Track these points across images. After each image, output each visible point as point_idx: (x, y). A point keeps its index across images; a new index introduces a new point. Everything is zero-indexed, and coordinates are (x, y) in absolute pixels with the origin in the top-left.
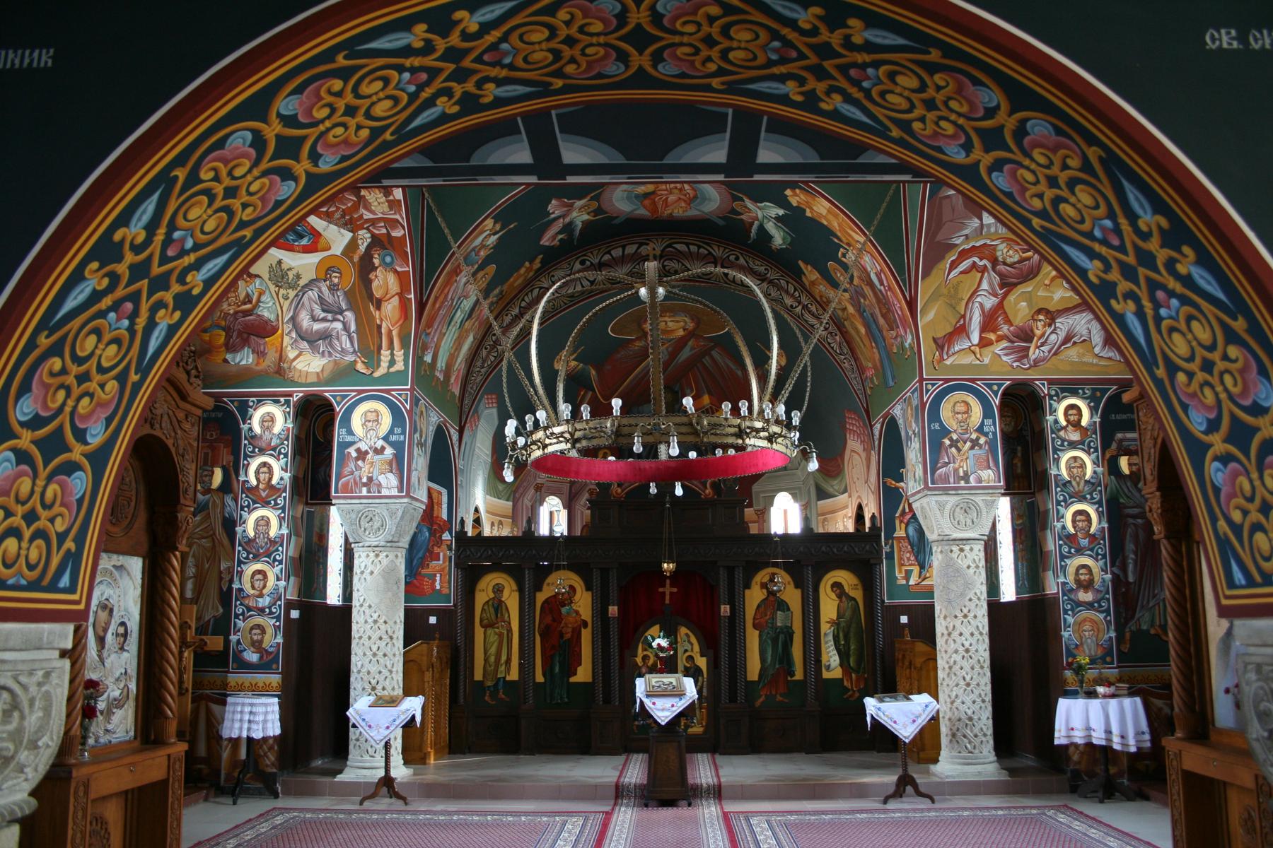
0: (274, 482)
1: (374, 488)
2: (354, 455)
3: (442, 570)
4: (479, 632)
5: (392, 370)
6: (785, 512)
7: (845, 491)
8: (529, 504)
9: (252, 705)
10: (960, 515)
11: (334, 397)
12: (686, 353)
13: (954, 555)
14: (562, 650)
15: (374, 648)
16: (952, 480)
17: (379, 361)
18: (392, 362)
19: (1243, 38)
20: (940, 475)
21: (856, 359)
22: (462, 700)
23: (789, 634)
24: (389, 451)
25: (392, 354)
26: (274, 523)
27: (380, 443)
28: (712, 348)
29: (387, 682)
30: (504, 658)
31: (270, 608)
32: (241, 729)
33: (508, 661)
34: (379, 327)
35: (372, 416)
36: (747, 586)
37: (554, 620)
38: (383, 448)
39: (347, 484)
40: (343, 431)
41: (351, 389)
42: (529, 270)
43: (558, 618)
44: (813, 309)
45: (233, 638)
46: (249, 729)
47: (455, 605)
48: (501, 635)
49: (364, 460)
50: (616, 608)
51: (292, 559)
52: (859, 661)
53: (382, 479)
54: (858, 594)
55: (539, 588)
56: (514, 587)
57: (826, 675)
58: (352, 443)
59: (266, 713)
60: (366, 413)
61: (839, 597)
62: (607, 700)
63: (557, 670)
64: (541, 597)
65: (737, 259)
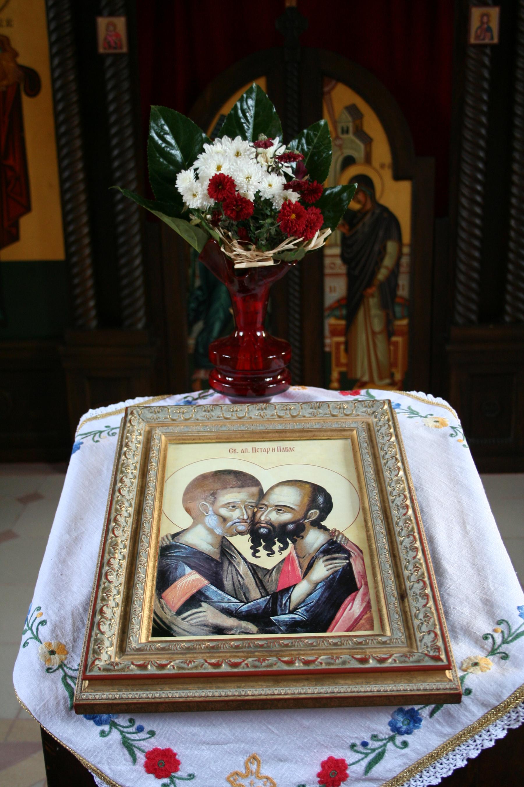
50: (120, 22)
62: (111, 317)
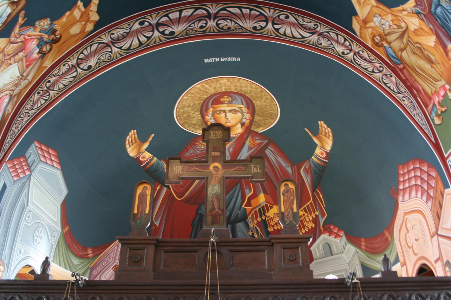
28: (266, 147)
42: (85, 16)
44: (365, 55)
65: (287, 17)
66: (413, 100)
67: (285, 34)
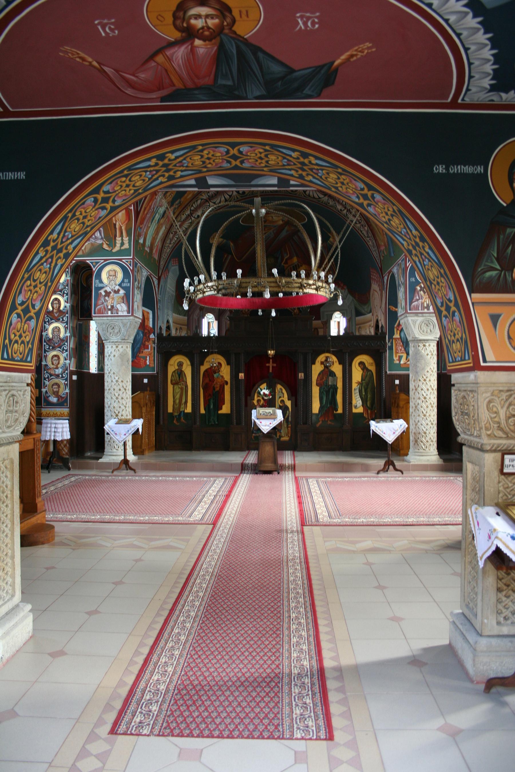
0: (61, 308)
1: (114, 311)
2: (103, 294)
3: (150, 354)
4: (170, 387)
5: (122, 248)
6: (339, 323)
7: (370, 312)
8: (197, 318)
9: (56, 424)
10: (424, 328)
11: (92, 263)
12: (284, 233)
13: (420, 348)
14: (215, 398)
15: (117, 395)
16: (420, 308)
17: (115, 243)
18: (122, 244)
19: (447, 169)
20: (414, 306)
21: (376, 240)
22: (161, 423)
23: (335, 389)
24: (122, 292)
25: (122, 240)
26: (62, 330)
27: (117, 287)
29: (124, 412)
30: (184, 401)
31: (62, 375)
32: (50, 436)
33: (186, 402)
34: (115, 225)
35: (112, 273)
36: (314, 363)
37: (210, 381)
38: (119, 290)
39: (100, 309)
40: (97, 281)
41: (100, 259)
43: (212, 379)
45: (44, 390)
46: (54, 436)
47: (157, 373)
48: (182, 389)
49: (109, 297)
51: (73, 349)
52: (372, 404)
53: (118, 306)
54: (372, 368)
55: (202, 364)
56: (189, 363)
57: (354, 411)
58: (102, 288)
59: (63, 428)
60: (109, 272)
61: (363, 369)
62: (239, 423)
63: (212, 407)
64: (203, 369)
66: (374, 241)
67: (309, 196)
